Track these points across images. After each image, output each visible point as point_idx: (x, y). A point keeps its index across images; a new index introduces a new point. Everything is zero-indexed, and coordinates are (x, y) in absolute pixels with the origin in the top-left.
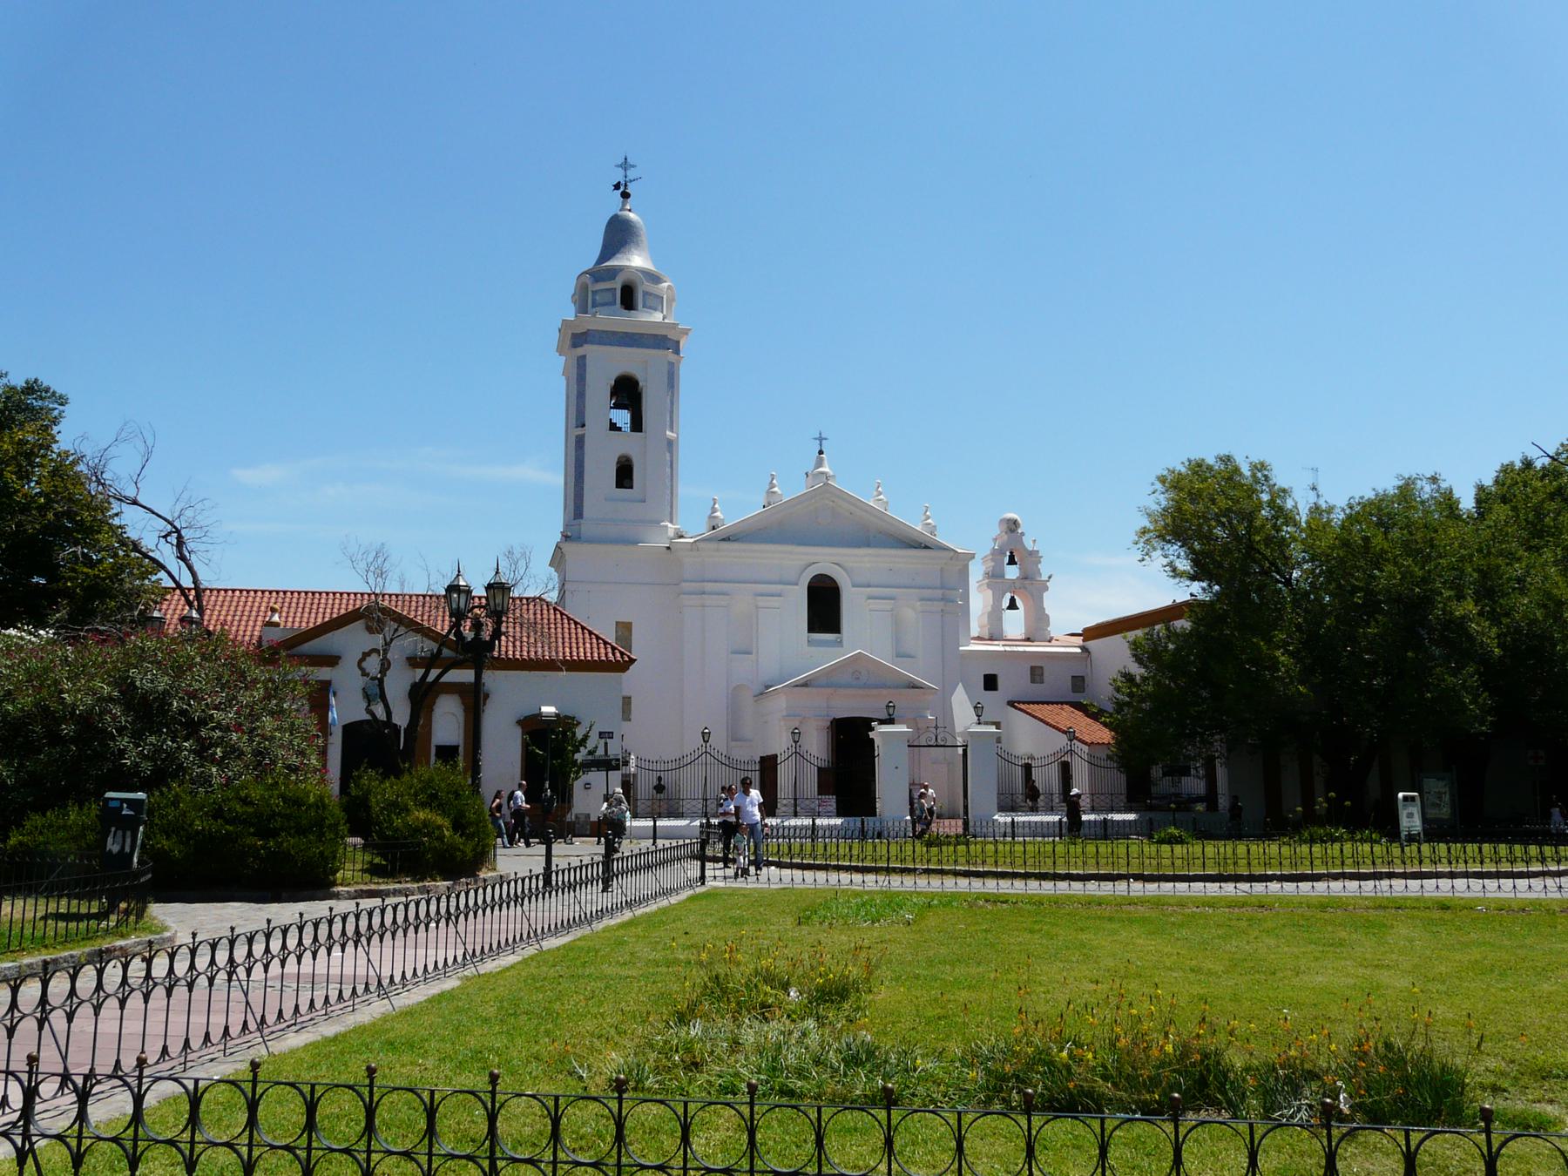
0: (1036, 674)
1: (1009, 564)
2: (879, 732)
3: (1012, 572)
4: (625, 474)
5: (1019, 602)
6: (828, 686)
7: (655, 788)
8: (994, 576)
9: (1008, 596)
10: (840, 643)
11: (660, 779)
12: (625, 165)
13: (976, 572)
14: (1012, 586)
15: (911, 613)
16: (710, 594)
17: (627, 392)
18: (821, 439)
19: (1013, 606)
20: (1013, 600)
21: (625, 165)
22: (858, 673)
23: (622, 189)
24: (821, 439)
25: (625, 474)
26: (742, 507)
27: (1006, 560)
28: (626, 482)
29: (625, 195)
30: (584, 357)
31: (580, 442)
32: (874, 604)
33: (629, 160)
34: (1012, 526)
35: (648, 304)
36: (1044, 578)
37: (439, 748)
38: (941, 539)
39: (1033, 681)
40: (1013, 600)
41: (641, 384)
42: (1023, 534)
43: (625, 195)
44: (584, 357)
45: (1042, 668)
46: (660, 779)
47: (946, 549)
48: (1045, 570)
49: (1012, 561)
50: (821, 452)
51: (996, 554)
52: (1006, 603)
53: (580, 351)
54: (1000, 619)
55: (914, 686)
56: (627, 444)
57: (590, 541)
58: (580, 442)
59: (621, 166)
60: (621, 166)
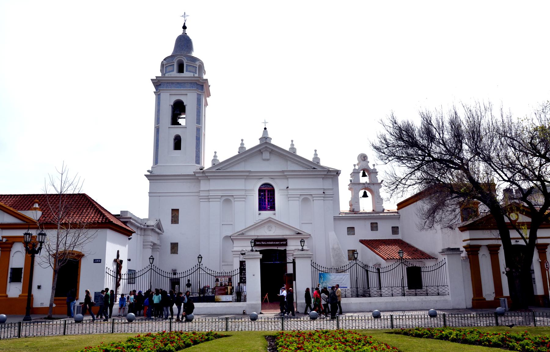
1: (362, 176)
3: (365, 180)
5: (368, 193)
7: (187, 285)
9: (363, 191)
11: (189, 281)
13: (344, 181)
19: (365, 195)
20: (365, 193)
21: (184, 15)
27: (361, 174)
33: (186, 14)
35: (189, 70)
36: (379, 181)
37: (12, 269)
39: (372, 230)
40: (365, 193)
41: (184, 104)
42: (368, 162)
46: (189, 281)
49: (364, 175)
50: (265, 129)
52: (361, 193)
54: (358, 202)
56: (176, 131)
59: (183, 16)
60: (183, 16)
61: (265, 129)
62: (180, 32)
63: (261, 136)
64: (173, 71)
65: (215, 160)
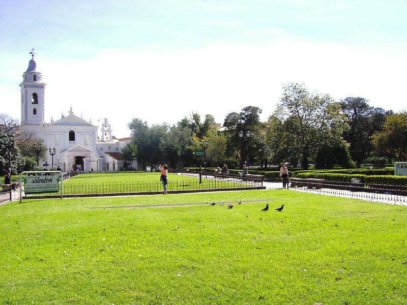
0: (110, 147)
3: (106, 129)
8: (103, 130)
12: (33, 50)
15: (87, 137)
17: (35, 96)
21: (33, 50)
22: (79, 150)
26: (57, 118)
29: (33, 56)
31: (26, 106)
32: (81, 136)
43: (33, 56)
48: (112, 128)
51: (103, 125)
52: (105, 134)
55: (89, 151)
56: (35, 106)
57: (29, 125)
58: (26, 106)
65: (52, 121)
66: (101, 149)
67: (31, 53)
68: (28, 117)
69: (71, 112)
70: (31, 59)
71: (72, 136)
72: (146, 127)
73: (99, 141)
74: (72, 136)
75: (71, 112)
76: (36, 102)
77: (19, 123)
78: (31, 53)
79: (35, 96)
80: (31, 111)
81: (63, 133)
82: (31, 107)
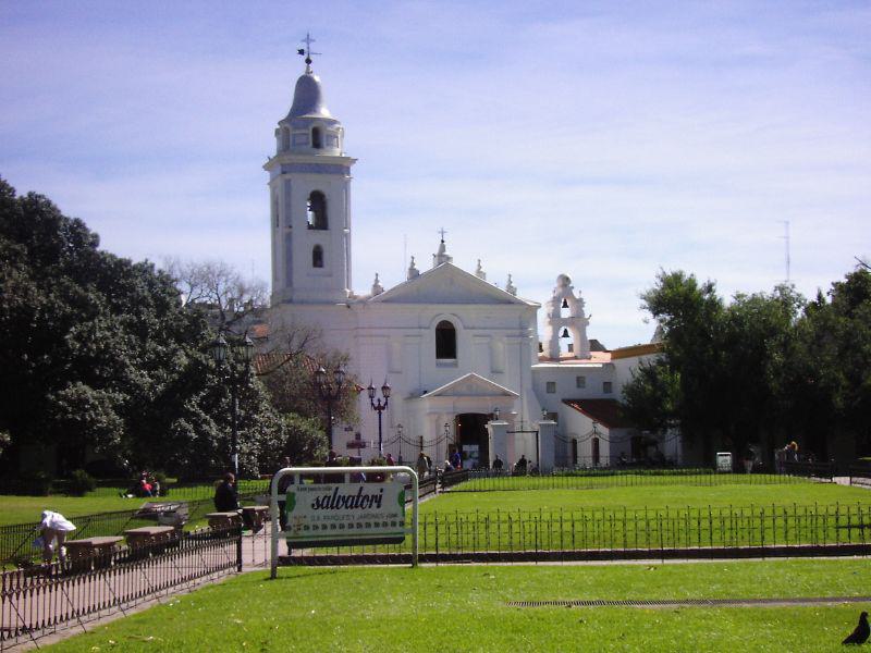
0: (580, 381)
2: (490, 426)
3: (566, 313)
4: (318, 257)
5: (570, 333)
6: (454, 395)
8: (555, 319)
9: (563, 329)
10: (456, 365)
12: (308, 40)
13: (542, 315)
14: (565, 322)
15: (501, 346)
16: (376, 336)
17: (318, 201)
18: (443, 233)
20: (566, 331)
22: (471, 389)
23: (305, 57)
24: (443, 233)
25: (318, 257)
26: (394, 278)
28: (318, 262)
29: (308, 61)
30: (290, 180)
31: (289, 238)
32: (478, 340)
34: (565, 281)
38: (520, 295)
39: (579, 386)
40: (566, 331)
43: (308, 61)
44: (290, 180)
45: (584, 378)
47: (521, 303)
48: (587, 311)
49: (565, 305)
50: (443, 241)
51: (556, 300)
52: (561, 333)
53: (287, 176)
55: (506, 394)
56: (319, 237)
58: (289, 238)
60: (303, 41)
61: (443, 241)
62: (301, 71)
63: (436, 252)
64: (307, 144)
65: (377, 288)
66: (551, 386)
67: (301, 52)
68: (296, 278)
69: (442, 257)
70: (302, 72)
71: (446, 343)
72: (714, 305)
73: (542, 360)
74: (446, 343)
75: (442, 257)
76: (321, 223)
77: (266, 297)
78: (301, 52)
79: (318, 201)
80: (304, 257)
81: (416, 331)
82: (305, 242)
